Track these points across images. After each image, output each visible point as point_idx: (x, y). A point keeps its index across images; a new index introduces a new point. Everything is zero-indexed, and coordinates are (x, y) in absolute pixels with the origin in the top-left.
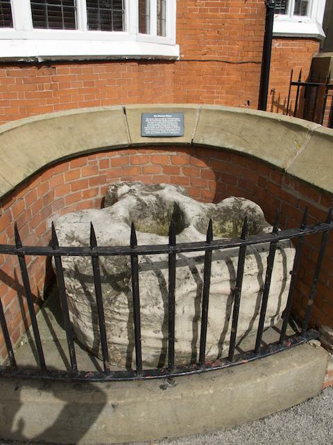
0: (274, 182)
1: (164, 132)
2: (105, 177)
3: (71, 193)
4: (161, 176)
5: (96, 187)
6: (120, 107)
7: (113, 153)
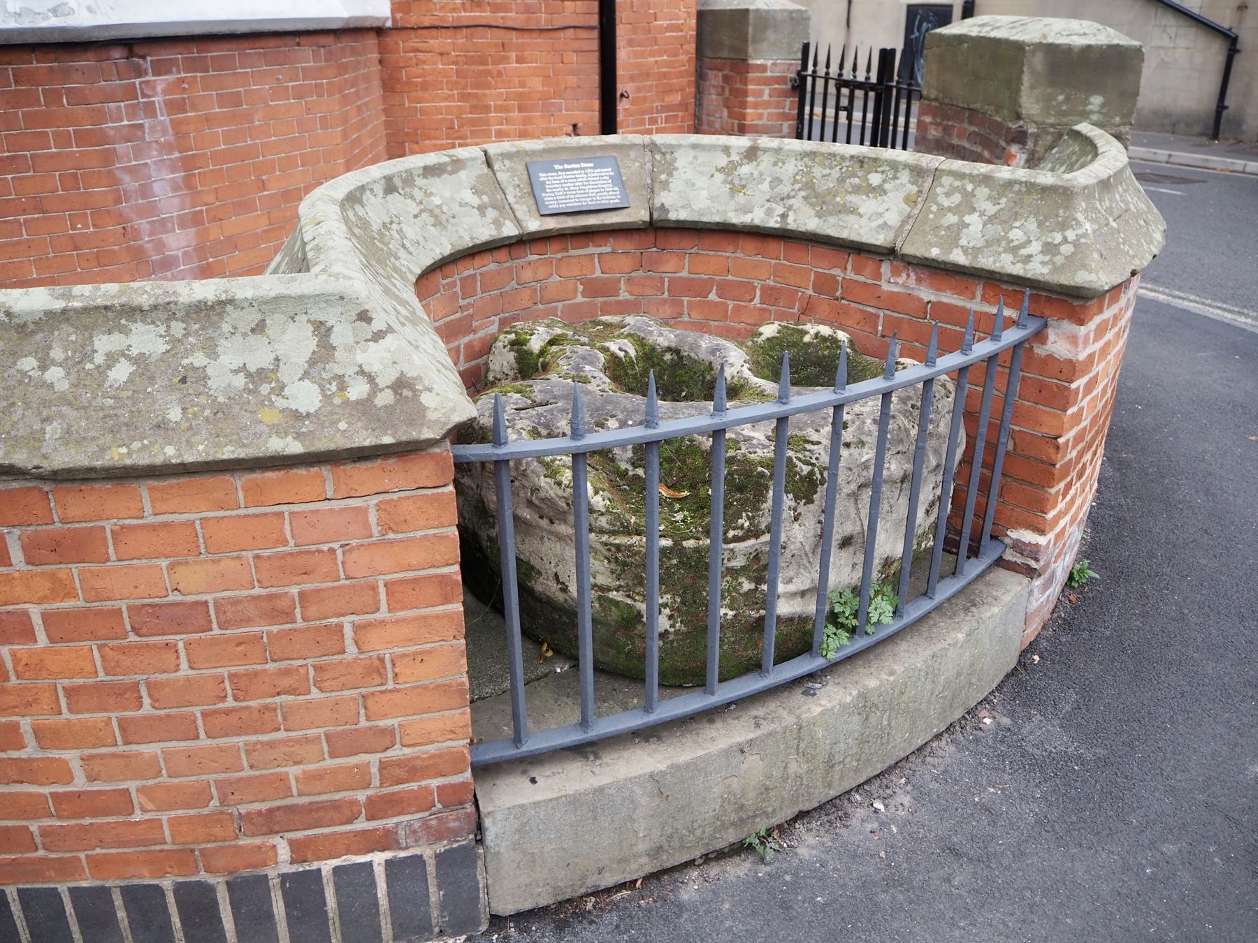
0: (861, 279)
4: (578, 305)
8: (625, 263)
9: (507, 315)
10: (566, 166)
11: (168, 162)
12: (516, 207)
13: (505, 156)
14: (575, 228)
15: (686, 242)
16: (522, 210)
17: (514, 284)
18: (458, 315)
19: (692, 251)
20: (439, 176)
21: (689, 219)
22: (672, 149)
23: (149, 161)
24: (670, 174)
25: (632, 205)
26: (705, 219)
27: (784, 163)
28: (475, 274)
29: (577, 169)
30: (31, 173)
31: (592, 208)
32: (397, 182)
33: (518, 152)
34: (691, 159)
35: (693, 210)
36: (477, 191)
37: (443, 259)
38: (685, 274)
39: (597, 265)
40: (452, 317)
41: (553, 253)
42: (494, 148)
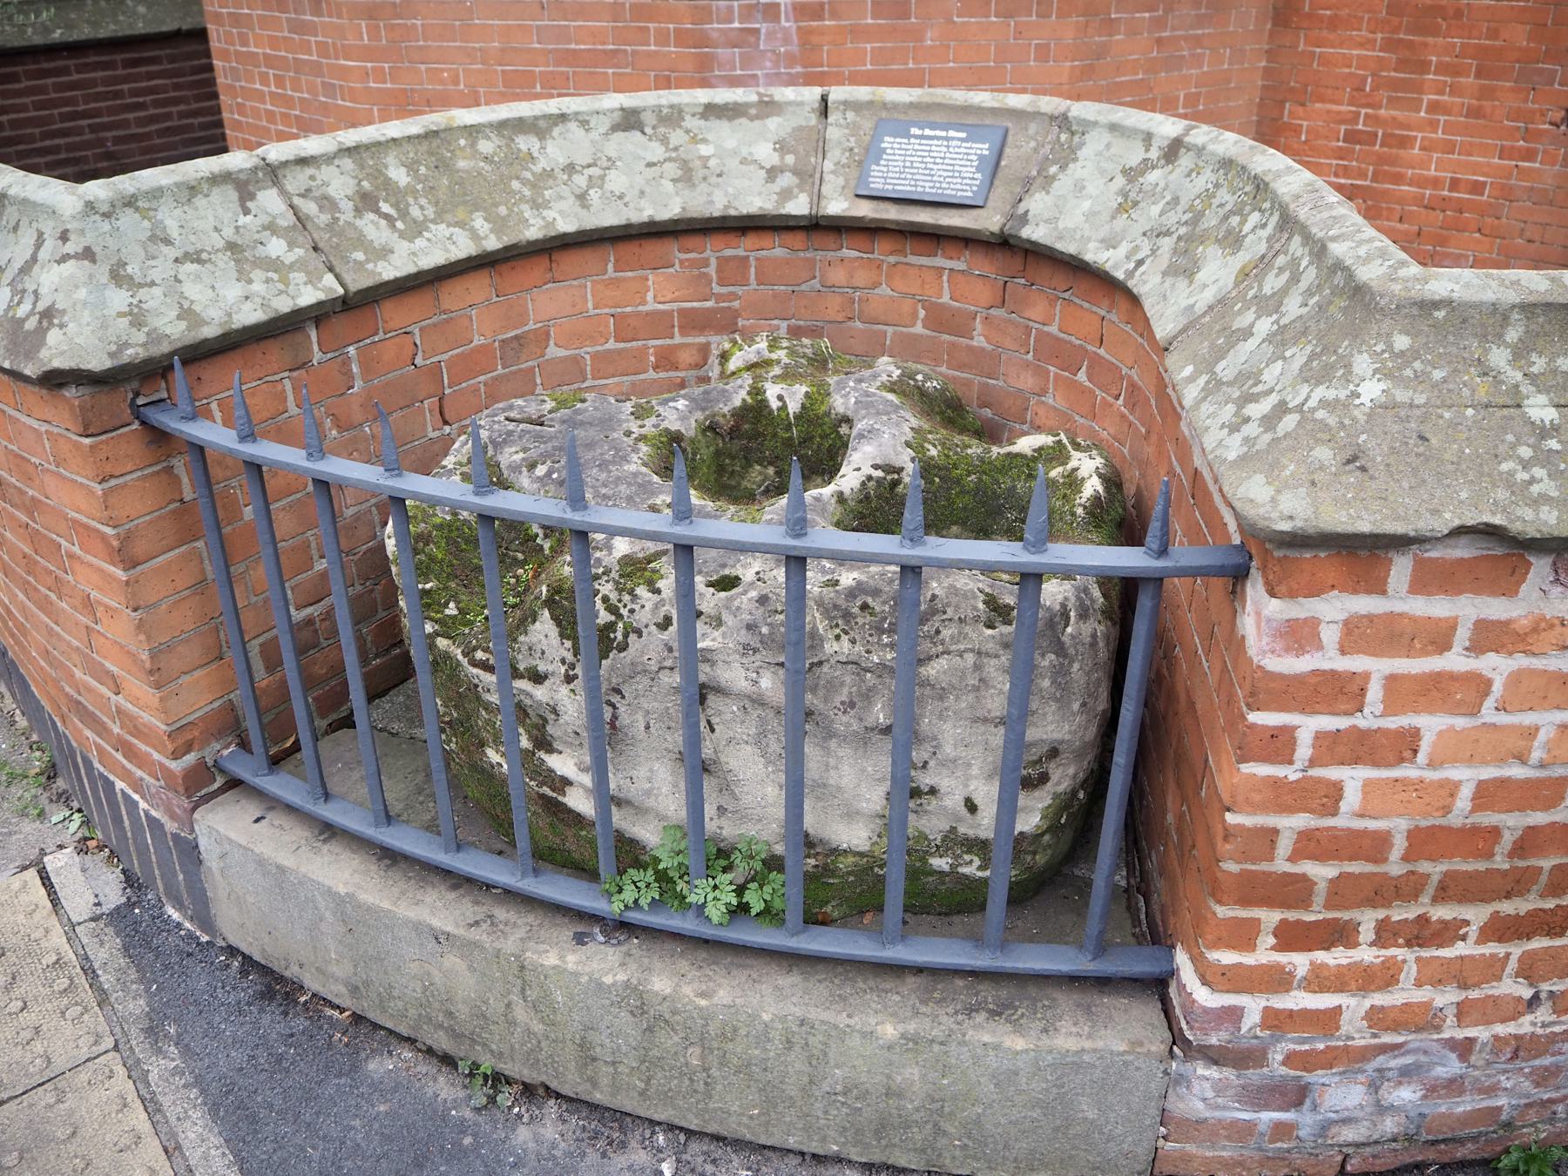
1: (927, 190)
2: (736, 314)
3: (611, 345)
5: (702, 340)
6: (813, 93)
7: (766, 240)
8: (983, 293)
9: (802, 323)
10: (927, 132)
11: (785, 77)
12: (827, 177)
13: (847, 105)
14: (897, 223)
15: (1060, 279)
16: (832, 184)
17: (815, 283)
18: (709, 304)
19: (1066, 295)
20: (730, 119)
21: (1041, 241)
22: (1087, 126)
23: (759, 73)
24: (1063, 168)
25: (990, 204)
26: (1059, 246)
27: (1198, 173)
28: (748, 257)
29: (938, 138)
30: (628, 70)
31: (927, 198)
32: (649, 119)
33: (871, 103)
34: (1101, 147)
35: (1056, 228)
36: (782, 147)
38: (1053, 329)
39: (946, 285)
40: (695, 304)
41: (883, 252)
42: (837, 93)
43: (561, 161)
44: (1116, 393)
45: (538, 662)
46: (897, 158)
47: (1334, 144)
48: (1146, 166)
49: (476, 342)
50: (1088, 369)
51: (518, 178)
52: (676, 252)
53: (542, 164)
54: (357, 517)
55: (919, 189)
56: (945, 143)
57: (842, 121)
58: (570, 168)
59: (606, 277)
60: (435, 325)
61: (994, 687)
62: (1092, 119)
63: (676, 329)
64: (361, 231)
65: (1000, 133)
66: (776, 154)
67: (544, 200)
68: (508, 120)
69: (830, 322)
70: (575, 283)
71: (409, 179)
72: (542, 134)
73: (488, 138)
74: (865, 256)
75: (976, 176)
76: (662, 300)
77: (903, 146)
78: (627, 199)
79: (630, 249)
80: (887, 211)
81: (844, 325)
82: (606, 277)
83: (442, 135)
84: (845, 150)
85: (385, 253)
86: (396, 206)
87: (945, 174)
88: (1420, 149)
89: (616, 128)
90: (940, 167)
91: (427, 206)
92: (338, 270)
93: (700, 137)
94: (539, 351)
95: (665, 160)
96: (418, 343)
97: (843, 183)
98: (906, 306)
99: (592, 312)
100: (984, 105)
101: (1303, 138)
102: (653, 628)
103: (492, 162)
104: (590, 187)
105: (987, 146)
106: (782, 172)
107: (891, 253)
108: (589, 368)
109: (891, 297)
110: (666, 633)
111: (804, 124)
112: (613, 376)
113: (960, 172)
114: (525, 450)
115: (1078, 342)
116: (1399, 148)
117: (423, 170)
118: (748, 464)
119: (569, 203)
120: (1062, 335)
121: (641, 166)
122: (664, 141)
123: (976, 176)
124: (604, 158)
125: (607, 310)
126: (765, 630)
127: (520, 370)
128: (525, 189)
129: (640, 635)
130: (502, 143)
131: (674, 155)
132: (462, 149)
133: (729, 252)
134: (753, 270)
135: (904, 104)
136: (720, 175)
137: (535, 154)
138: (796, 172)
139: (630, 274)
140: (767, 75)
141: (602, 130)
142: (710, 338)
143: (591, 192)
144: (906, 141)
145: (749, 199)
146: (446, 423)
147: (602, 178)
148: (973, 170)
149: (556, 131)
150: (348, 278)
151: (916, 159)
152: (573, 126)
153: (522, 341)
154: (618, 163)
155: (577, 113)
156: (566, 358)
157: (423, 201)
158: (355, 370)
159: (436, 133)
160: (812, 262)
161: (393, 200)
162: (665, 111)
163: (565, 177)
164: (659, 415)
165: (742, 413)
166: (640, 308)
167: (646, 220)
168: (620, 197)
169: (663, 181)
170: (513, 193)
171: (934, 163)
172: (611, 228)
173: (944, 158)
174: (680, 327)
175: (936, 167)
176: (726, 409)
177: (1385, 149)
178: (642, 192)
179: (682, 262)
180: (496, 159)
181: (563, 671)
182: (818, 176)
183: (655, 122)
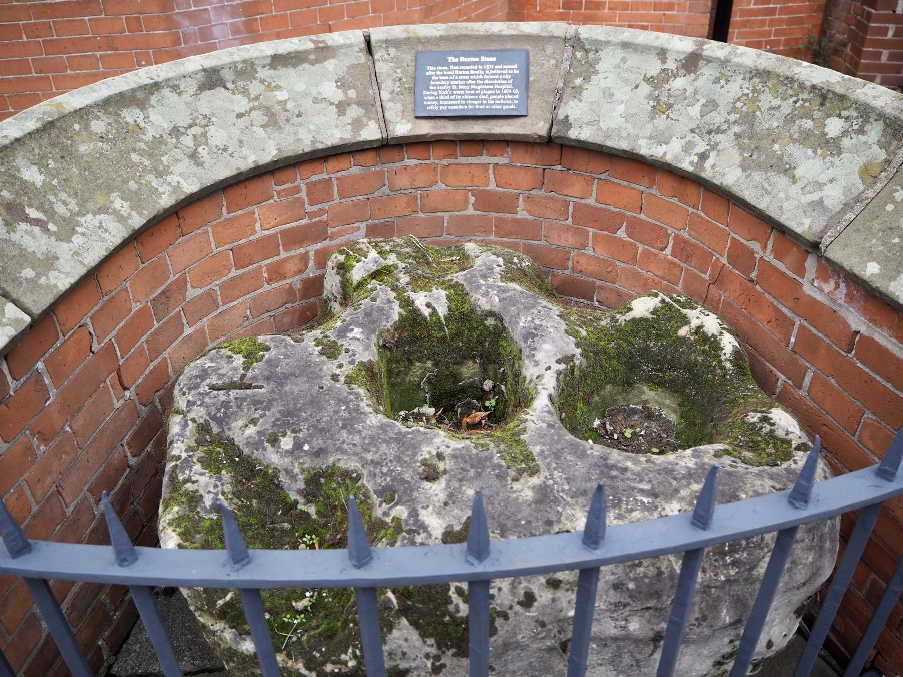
0: (781, 266)
1: (476, 106)
2: (326, 224)
3: (234, 273)
4: (469, 218)
5: (302, 250)
6: (355, 36)
7: (344, 162)
8: (525, 179)
9: (377, 221)
10: (462, 59)
11: (228, 8)
12: (387, 105)
13: (388, 43)
14: (455, 135)
15: (596, 165)
16: (393, 111)
17: (386, 189)
18: (304, 222)
19: (603, 176)
20: (295, 66)
21: (591, 140)
22: (599, 45)
23: (209, 7)
24: (587, 79)
25: (531, 113)
26: (609, 143)
27: (728, 81)
28: (330, 179)
29: (474, 63)
30: (103, 16)
31: (478, 114)
32: (228, 75)
33: (408, 39)
34: (618, 61)
35: (600, 129)
36: (342, 84)
37: (240, 174)
38: (592, 201)
39: (492, 176)
40: (294, 224)
41: (438, 159)
42: (378, 34)
43: (165, 126)
44: (663, 246)
45: (399, 662)
46: (443, 83)
47: (557, 11)
48: (666, 76)
49: (134, 310)
50: (626, 227)
51: (135, 151)
52: (274, 187)
53: (151, 133)
54: (77, 510)
55: (470, 107)
56: (481, 67)
57: (386, 56)
58: (175, 132)
59: (222, 219)
60: (101, 309)
61: (801, 564)
62: (603, 39)
63: (281, 247)
64: (20, 245)
65: (524, 55)
66: (340, 91)
67: (164, 166)
68: (111, 97)
69: (399, 217)
70: (199, 231)
71: (42, 177)
72: (143, 105)
73: (98, 118)
74: (423, 162)
75: (514, 91)
76: (268, 226)
77: (446, 73)
78: (230, 150)
79: (237, 193)
80: (445, 127)
81: (410, 217)
82: (222, 219)
83: (58, 124)
84: (395, 80)
85: (50, 262)
86: (40, 208)
87: (488, 92)
88: (609, 9)
89: (202, 88)
90: (482, 87)
91: (68, 199)
92: (14, 296)
93: (274, 84)
94: (181, 297)
95: (251, 110)
96: (92, 331)
97: (402, 108)
98: (459, 196)
99: (215, 251)
100: (503, 33)
101: (538, 9)
102: (518, 608)
103: (108, 140)
104: (197, 146)
105: (516, 66)
106: (348, 105)
107: (444, 158)
108: (219, 297)
109: (446, 191)
110: (533, 609)
111: (355, 62)
112: (239, 297)
113: (500, 89)
114: (254, 422)
115: (617, 210)
116: (596, 9)
117: (51, 162)
118: (411, 362)
119: (185, 165)
120: (599, 205)
121: (232, 118)
122: (245, 92)
123: (514, 91)
124: (201, 117)
125: (227, 247)
126: (631, 586)
127: (171, 318)
128: (144, 160)
129: (506, 617)
130: (111, 120)
131: (256, 104)
132: (78, 134)
133: (315, 178)
134: (335, 188)
135: (436, 37)
136: (299, 116)
137: (142, 125)
138: (360, 104)
139: (240, 212)
140: (215, 7)
141: (192, 91)
142: (307, 248)
143: (200, 150)
144: (446, 68)
145: (329, 132)
146: (126, 389)
147: (204, 134)
148: (510, 87)
149: (153, 99)
150: (27, 301)
151: (459, 82)
152: (166, 92)
153: (167, 295)
154: (213, 119)
155: (167, 80)
156: (201, 295)
157: (63, 196)
158: (47, 382)
159: (52, 124)
160: (382, 172)
161: (36, 202)
162: (240, 66)
163: (174, 141)
164: (347, 351)
165: (401, 325)
166: (252, 237)
167: (252, 166)
168: (225, 150)
169: (255, 128)
170: (135, 166)
171: (477, 84)
172: (226, 179)
173: (470, 75)
174: (283, 245)
175: (478, 87)
176: (389, 326)
177: (588, 11)
178: (241, 142)
179: (279, 193)
180: (110, 136)
181: (429, 665)
182: (378, 104)
183: (233, 78)
